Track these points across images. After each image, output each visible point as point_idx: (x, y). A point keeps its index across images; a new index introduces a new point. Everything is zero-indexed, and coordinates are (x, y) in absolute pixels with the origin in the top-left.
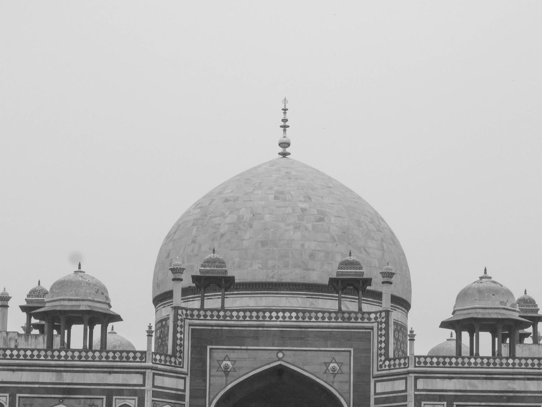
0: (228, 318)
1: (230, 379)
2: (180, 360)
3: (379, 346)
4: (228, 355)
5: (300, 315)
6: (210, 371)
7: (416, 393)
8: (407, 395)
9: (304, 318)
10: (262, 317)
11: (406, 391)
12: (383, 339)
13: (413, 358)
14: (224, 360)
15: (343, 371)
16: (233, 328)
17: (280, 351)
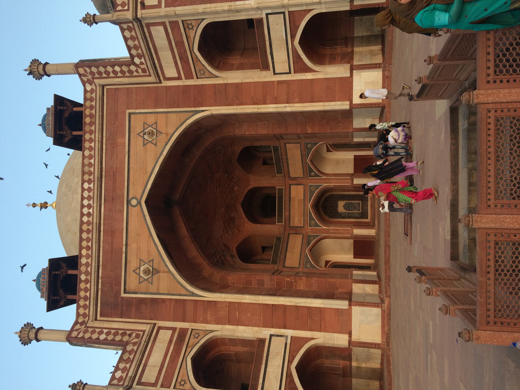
0: (89, 269)
1: (162, 268)
2: (134, 335)
3: (119, 75)
4: (134, 269)
5: (86, 177)
6: (152, 294)
7: (163, 5)
8: (170, 23)
9: (90, 173)
10: (89, 225)
11: (163, 24)
12: (109, 69)
13: (118, 13)
14: (139, 274)
15: (154, 122)
16: (101, 263)
17: (128, 202)
